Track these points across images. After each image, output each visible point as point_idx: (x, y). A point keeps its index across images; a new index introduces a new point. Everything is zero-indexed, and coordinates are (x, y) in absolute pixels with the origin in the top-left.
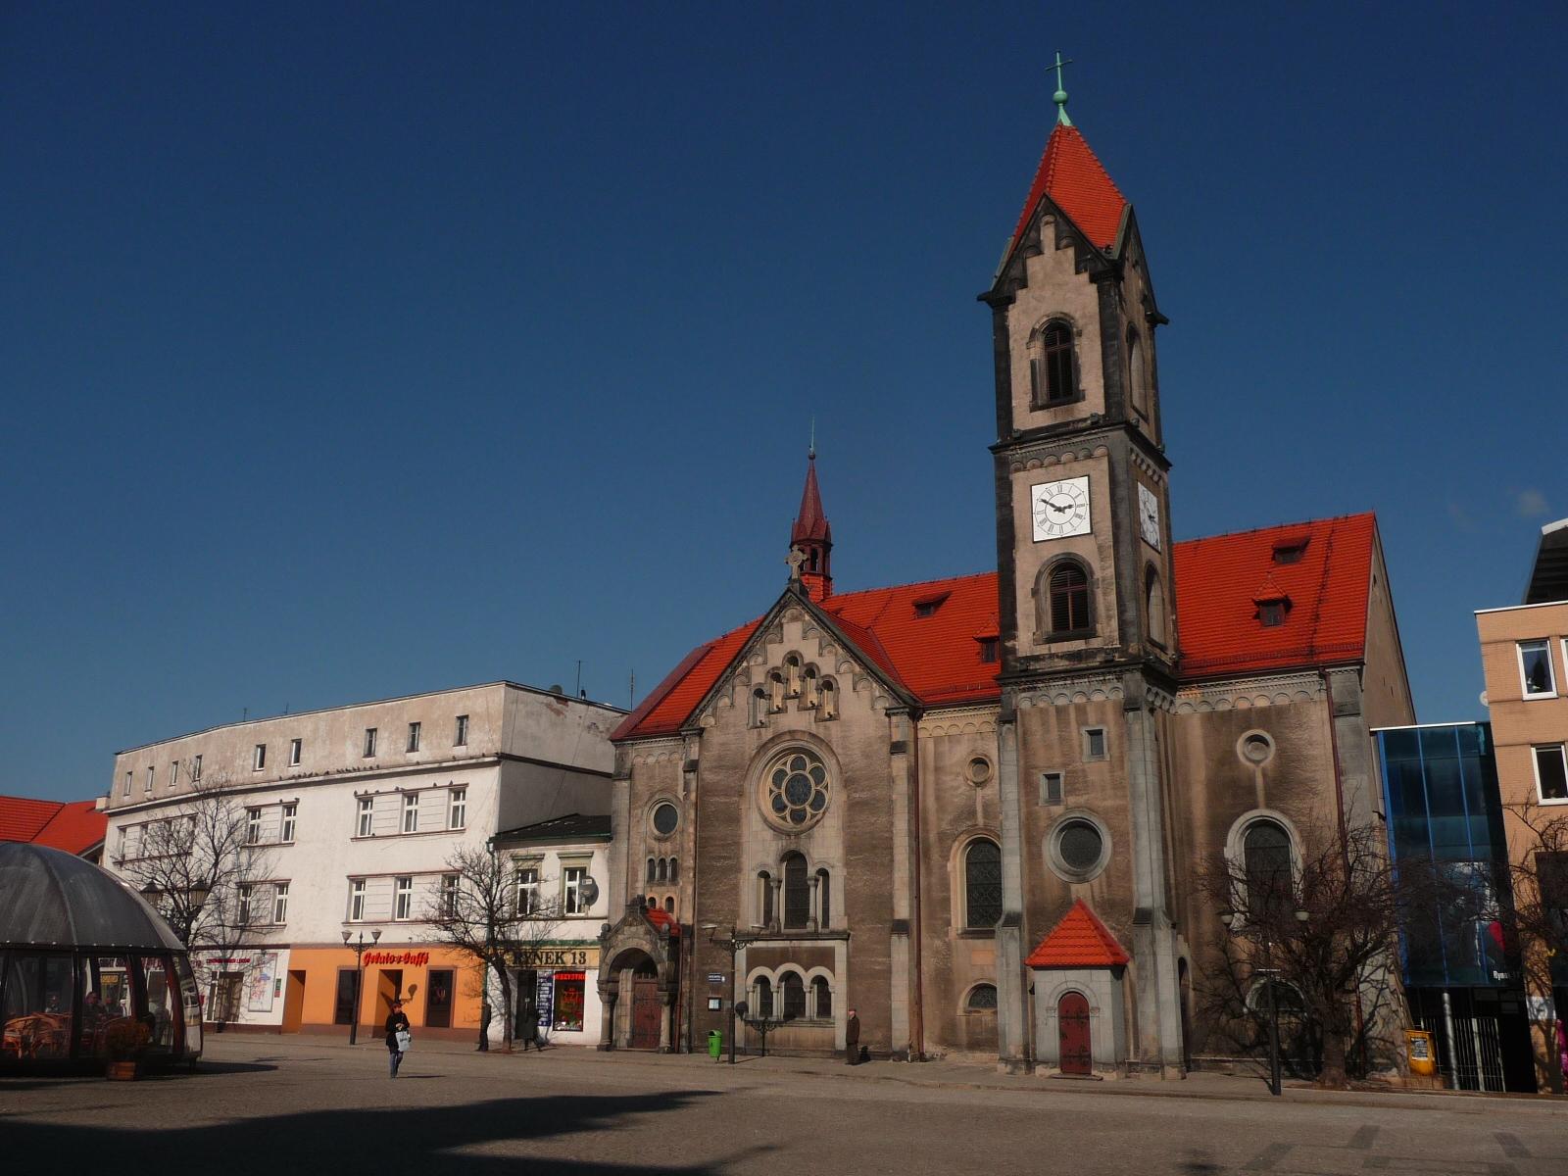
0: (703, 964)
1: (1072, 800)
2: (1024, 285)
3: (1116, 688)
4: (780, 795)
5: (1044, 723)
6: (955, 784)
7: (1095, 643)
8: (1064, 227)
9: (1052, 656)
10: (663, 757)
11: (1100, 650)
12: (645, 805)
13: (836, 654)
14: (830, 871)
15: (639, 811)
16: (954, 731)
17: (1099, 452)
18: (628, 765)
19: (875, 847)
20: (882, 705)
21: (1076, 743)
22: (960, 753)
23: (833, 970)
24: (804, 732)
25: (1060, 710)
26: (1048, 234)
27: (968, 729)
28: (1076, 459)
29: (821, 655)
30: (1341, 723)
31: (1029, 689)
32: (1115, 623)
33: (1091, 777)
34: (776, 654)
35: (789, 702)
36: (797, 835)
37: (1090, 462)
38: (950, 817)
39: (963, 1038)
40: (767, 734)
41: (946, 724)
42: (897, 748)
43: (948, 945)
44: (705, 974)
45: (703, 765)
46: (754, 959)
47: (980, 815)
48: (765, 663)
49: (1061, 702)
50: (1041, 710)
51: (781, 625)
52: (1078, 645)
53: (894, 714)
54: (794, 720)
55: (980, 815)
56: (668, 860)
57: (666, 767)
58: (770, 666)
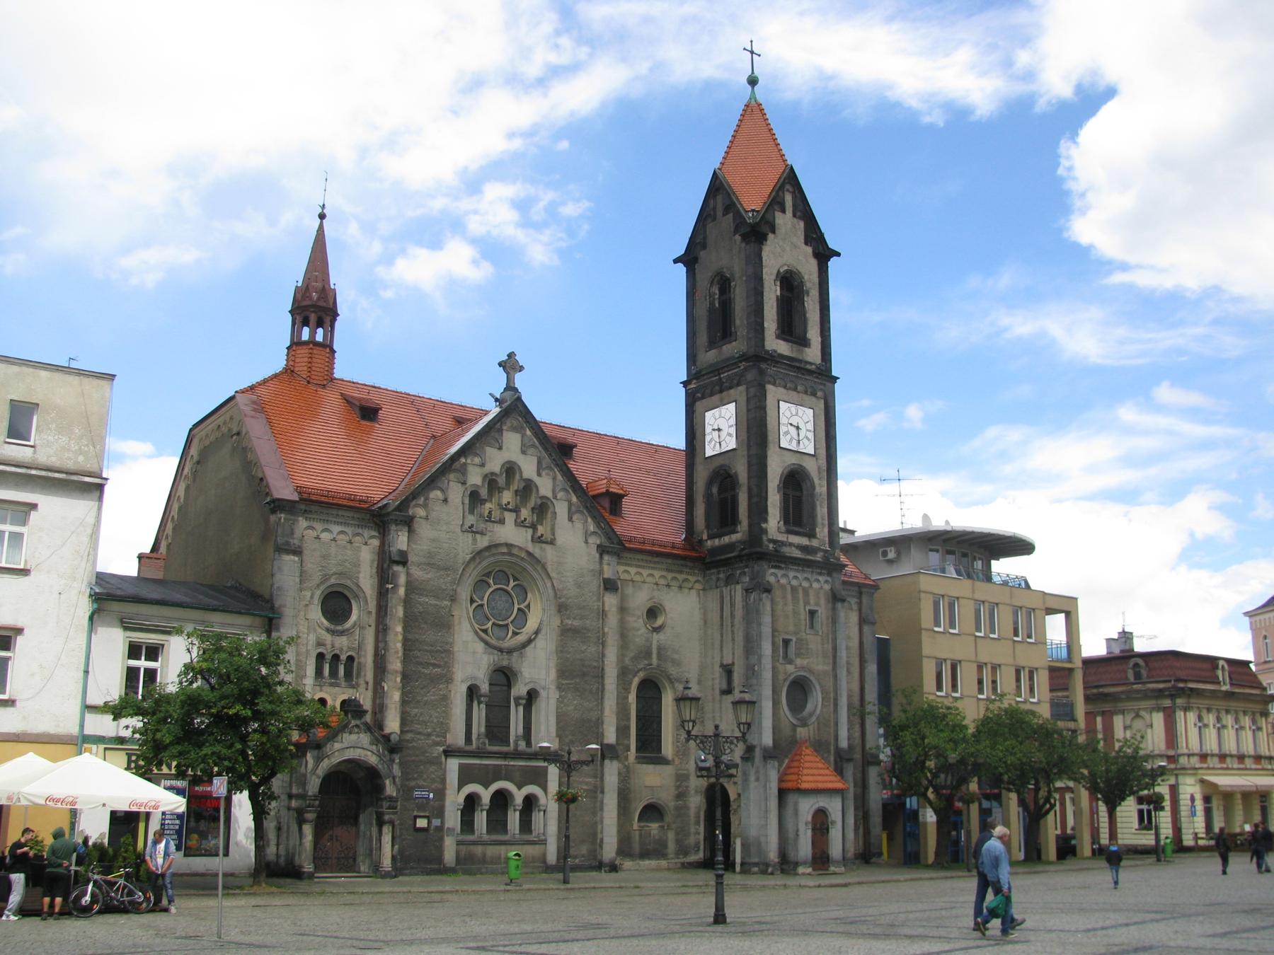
1: (799, 661)
2: (774, 232)
3: (826, 582)
4: (482, 605)
5: (784, 597)
7: (815, 543)
9: (791, 545)
10: (341, 536)
12: (318, 586)
13: (554, 479)
15: (308, 594)
16: (637, 578)
18: (298, 534)
19: (584, 674)
21: (802, 617)
22: (640, 599)
23: (545, 790)
24: (521, 548)
25: (794, 589)
27: (650, 579)
28: (806, 393)
29: (539, 474)
30: (866, 629)
31: (774, 567)
32: (826, 530)
33: (812, 646)
34: (495, 460)
36: (510, 651)
37: (814, 399)
38: (632, 654)
39: (636, 847)
40: (483, 542)
41: (633, 570)
42: (610, 585)
43: (627, 767)
44: (412, 789)
45: (412, 558)
46: (466, 776)
47: (654, 656)
48: (483, 465)
49: (794, 583)
50: (783, 586)
51: (500, 431)
52: (804, 541)
53: (608, 553)
54: (510, 533)
55: (654, 656)
56: (343, 657)
57: (345, 547)
58: (487, 469)
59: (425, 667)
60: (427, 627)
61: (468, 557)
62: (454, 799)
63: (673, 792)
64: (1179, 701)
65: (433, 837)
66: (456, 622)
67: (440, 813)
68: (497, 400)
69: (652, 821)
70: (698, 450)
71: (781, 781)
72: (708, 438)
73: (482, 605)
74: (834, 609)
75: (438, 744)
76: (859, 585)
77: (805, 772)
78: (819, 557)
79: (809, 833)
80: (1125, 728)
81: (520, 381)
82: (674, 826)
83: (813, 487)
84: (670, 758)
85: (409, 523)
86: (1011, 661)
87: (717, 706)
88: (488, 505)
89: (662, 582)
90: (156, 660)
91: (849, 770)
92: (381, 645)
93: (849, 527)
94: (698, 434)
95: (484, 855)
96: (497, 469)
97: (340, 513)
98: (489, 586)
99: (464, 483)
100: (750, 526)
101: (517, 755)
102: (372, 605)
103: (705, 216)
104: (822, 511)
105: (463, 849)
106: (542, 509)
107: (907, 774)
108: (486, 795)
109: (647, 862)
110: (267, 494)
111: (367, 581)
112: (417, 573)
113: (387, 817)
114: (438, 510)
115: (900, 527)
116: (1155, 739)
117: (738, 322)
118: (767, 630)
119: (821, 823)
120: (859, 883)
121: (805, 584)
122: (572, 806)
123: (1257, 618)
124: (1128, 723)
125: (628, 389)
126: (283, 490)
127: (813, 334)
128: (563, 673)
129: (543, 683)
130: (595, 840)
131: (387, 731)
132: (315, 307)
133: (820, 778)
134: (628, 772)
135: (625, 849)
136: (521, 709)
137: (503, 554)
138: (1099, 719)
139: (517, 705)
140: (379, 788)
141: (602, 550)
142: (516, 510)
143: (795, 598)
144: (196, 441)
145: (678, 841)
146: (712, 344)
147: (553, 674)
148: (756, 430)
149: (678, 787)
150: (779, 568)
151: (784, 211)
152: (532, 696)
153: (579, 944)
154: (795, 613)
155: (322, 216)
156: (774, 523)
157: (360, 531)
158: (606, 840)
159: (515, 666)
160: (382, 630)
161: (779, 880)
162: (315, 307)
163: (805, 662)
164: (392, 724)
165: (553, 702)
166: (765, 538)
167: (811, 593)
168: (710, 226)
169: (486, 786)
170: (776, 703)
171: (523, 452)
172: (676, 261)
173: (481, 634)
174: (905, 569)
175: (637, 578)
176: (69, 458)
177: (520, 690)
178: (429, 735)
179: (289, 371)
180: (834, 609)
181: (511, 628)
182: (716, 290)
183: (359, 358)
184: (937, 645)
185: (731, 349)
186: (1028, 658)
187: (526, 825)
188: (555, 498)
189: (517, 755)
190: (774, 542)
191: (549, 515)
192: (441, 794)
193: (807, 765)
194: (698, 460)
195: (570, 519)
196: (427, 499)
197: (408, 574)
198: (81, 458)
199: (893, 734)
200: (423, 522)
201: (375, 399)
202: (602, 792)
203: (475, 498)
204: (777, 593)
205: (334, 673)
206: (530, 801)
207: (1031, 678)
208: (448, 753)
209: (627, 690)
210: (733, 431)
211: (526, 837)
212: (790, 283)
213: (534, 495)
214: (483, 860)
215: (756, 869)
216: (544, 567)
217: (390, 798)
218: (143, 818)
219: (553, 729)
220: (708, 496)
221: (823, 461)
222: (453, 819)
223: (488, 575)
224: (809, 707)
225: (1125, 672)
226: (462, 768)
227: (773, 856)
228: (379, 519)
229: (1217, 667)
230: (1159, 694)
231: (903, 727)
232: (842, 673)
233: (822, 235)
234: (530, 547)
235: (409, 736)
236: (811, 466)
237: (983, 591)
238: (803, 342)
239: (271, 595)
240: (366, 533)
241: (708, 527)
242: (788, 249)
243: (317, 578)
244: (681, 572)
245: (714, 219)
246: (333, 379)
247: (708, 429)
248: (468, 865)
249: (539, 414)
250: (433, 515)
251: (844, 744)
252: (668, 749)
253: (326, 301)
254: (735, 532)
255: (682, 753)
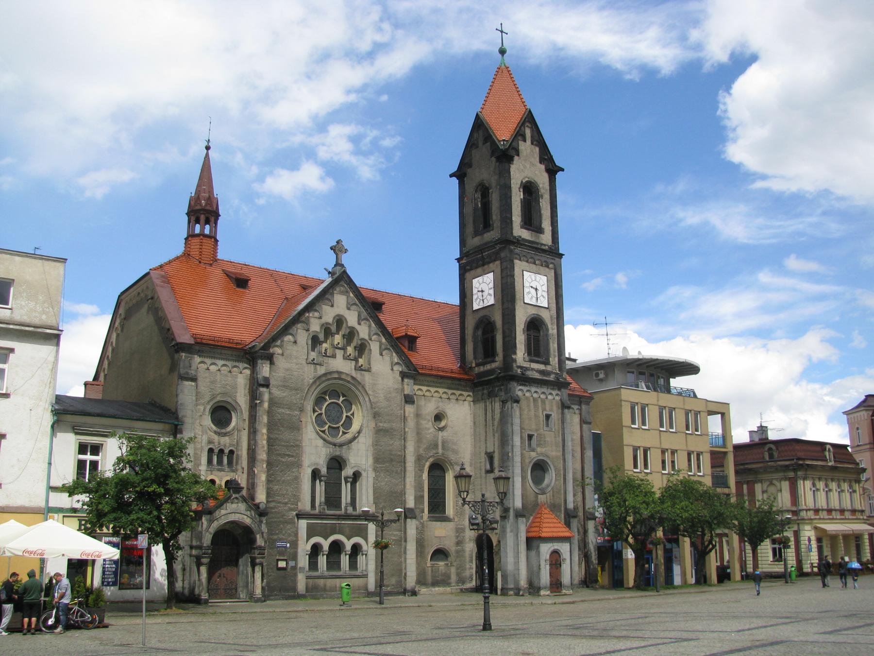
0: (272, 534)
1: (539, 450)
2: (518, 155)
3: (557, 395)
4: (321, 414)
5: (528, 406)
6: (427, 426)
7: (549, 368)
8: (535, 134)
9: (533, 369)
11: (552, 373)
13: (370, 326)
14: (363, 472)
15: (202, 408)
17: (551, 266)
18: (194, 367)
19: (392, 460)
20: (398, 369)
22: (430, 408)
23: (366, 539)
24: (347, 375)
25: (535, 400)
26: (528, 132)
29: (359, 324)
32: (557, 359)
33: (548, 439)
34: (328, 314)
35: (337, 351)
36: (341, 445)
37: (547, 269)
39: (429, 579)
40: (321, 371)
41: (424, 388)
42: (409, 400)
44: (275, 541)
48: (320, 318)
50: (527, 398)
51: (332, 294)
52: (542, 367)
54: (340, 364)
56: (227, 451)
57: (226, 375)
58: (323, 320)
59: (283, 457)
60: (283, 429)
61: (311, 381)
62: (304, 547)
63: (454, 540)
64: (799, 473)
65: (288, 574)
66: (304, 425)
67: (294, 557)
68: (329, 273)
69: (442, 560)
70: (468, 305)
71: (528, 532)
72: (475, 297)
73: (321, 414)
74: (563, 413)
75: (292, 510)
76: (580, 397)
77: (544, 525)
78: (552, 378)
79: (548, 567)
80: (763, 492)
81: (345, 259)
82: (455, 564)
83: (547, 330)
84: (451, 517)
85: (270, 358)
86: (685, 448)
87: (484, 481)
88: (325, 345)
89: (444, 396)
90: (98, 455)
91: (575, 523)
92: (252, 442)
93: (572, 357)
94: (468, 294)
95: (325, 585)
96: (330, 320)
97: (223, 351)
98: (326, 400)
99: (308, 330)
100: (505, 357)
101: (347, 517)
102: (246, 415)
103: (471, 145)
104: (553, 346)
105: (310, 581)
106: (362, 348)
107: (614, 526)
108: (326, 544)
109: (437, 589)
110: (173, 340)
111: (242, 399)
112: (276, 392)
113: (258, 561)
114: (291, 349)
115: (606, 356)
116: (784, 499)
117: (494, 217)
118: (517, 428)
119: (556, 560)
120: (582, 601)
121: (543, 396)
122: (384, 551)
123: (852, 416)
124: (765, 488)
125: (420, 265)
126: (185, 338)
127: (546, 225)
128: (377, 460)
129: (364, 467)
130: (401, 573)
131: (257, 501)
132: (203, 211)
133: (555, 530)
134: (423, 527)
135: (421, 581)
136: (349, 485)
137: (335, 378)
138: (745, 486)
139: (346, 482)
140: (254, 541)
141: (403, 375)
142: (344, 349)
143: (536, 406)
144: (123, 304)
145: (458, 574)
146: (476, 233)
147: (371, 461)
148: (507, 292)
149: (457, 537)
150: (525, 385)
151: (525, 141)
152: (356, 476)
153: (391, 646)
154: (536, 416)
155: (208, 148)
156: (520, 355)
157: (237, 364)
158: (408, 574)
159: (344, 455)
160: (253, 432)
161: (527, 599)
162: (203, 211)
163: (543, 450)
164: (261, 497)
165: (371, 480)
166: (514, 365)
167: (547, 402)
168: (474, 152)
169: (326, 538)
170: (524, 478)
171: (349, 309)
172: (451, 176)
173: (321, 434)
174: (611, 385)
175: (427, 394)
176: (35, 317)
177: (348, 472)
178: (286, 503)
179: (186, 255)
180: (563, 413)
181: (341, 429)
182: (478, 195)
183: (234, 246)
184: (634, 437)
185: (492, 235)
186: (697, 445)
187: (353, 565)
188: (371, 339)
189: (347, 517)
190: (521, 367)
191: (367, 351)
192: (295, 544)
193: (545, 520)
194: (468, 312)
195: (381, 354)
196: (282, 341)
197: (270, 393)
198: (44, 317)
199: (605, 498)
200: (280, 357)
201: (246, 273)
202: (406, 541)
203: (315, 341)
204: (523, 403)
205: (220, 462)
206: (356, 549)
207: (698, 459)
208: (300, 516)
209: (422, 471)
210: (492, 292)
211: (354, 573)
212: (529, 189)
213: (356, 337)
214: (324, 589)
215: (511, 592)
216: (363, 387)
217: (260, 548)
218: (90, 563)
219: (371, 498)
220: (474, 337)
221: (554, 312)
222: (303, 561)
223: (325, 393)
224: (546, 481)
225: (763, 454)
226: (309, 527)
227: (523, 583)
228: (251, 355)
229: (825, 450)
230: (786, 468)
231: (611, 494)
232: (569, 457)
233: (551, 157)
234: (354, 374)
235: (272, 505)
236: (546, 316)
237: (665, 399)
238: (539, 230)
239: (176, 410)
240: (242, 365)
241: (475, 358)
242: (528, 166)
243: (207, 398)
244: (458, 389)
245: (477, 147)
246: (216, 260)
247: (475, 291)
248: (314, 592)
249: (359, 283)
250: (287, 353)
251: (571, 506)
252: (450, 510)
253: (211, 206)
254: (494, 361)
255: (460, 513)
